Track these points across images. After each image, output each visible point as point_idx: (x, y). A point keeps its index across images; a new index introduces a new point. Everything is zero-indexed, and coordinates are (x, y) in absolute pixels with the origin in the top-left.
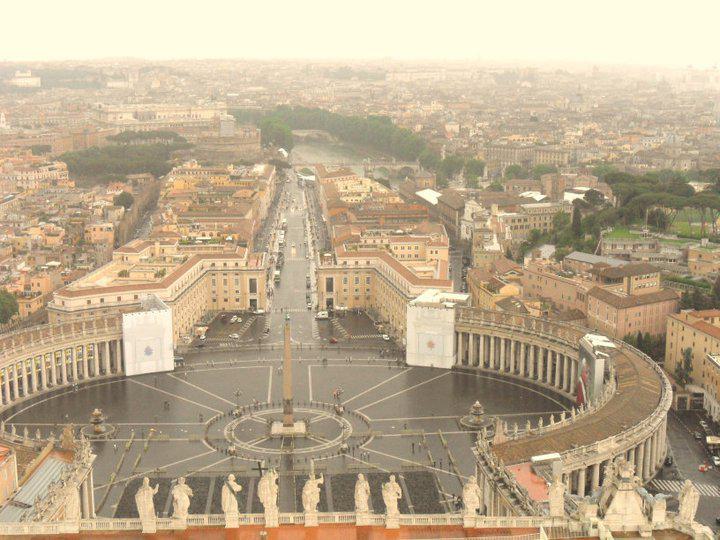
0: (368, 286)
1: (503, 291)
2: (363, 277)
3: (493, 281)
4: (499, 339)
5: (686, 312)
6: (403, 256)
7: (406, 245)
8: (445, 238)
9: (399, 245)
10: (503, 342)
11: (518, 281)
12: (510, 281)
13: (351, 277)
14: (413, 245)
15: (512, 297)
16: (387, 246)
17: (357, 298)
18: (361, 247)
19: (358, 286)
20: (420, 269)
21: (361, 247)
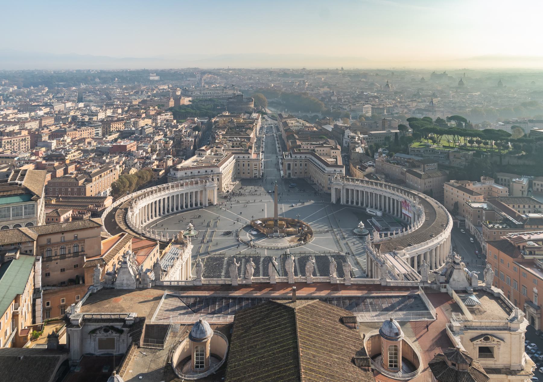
0: (306, 167)
1: (366, 170)
2: (303, 163)
3: (362, 166)
4: (368, 192)
5: (453, 181)
6: (320, 154)
7: (322, 149)
8: (339, 147)
9: (319, 149)
10: (369, 194)
11: (373, 166)
12: (370, 166)
13: (298, 163)
14: (325, 149)
15: (371, 173)
16: (314, 150)
17: (301, 173)
18: (302, 150)
19: (301, 167)
20: (330, 160)
21: (302, 150)
